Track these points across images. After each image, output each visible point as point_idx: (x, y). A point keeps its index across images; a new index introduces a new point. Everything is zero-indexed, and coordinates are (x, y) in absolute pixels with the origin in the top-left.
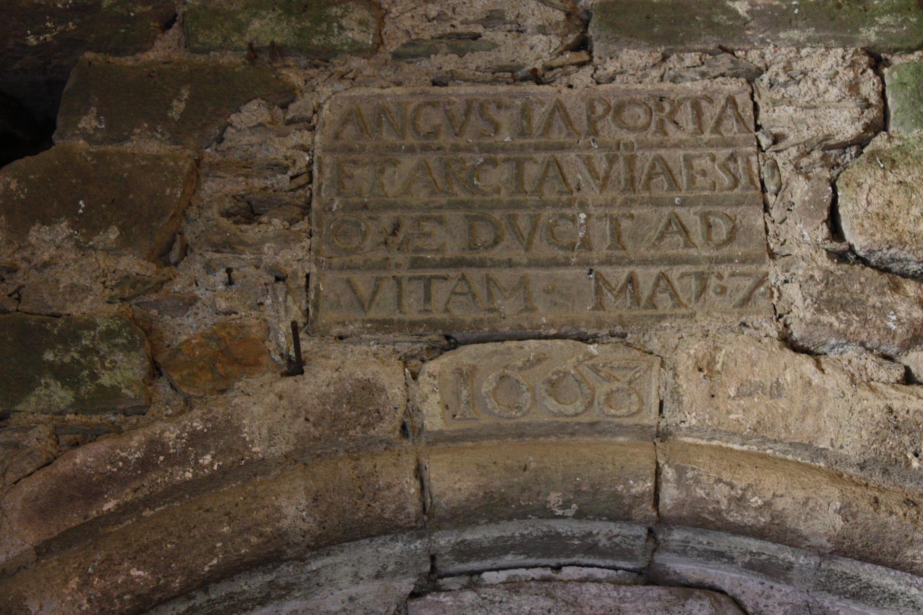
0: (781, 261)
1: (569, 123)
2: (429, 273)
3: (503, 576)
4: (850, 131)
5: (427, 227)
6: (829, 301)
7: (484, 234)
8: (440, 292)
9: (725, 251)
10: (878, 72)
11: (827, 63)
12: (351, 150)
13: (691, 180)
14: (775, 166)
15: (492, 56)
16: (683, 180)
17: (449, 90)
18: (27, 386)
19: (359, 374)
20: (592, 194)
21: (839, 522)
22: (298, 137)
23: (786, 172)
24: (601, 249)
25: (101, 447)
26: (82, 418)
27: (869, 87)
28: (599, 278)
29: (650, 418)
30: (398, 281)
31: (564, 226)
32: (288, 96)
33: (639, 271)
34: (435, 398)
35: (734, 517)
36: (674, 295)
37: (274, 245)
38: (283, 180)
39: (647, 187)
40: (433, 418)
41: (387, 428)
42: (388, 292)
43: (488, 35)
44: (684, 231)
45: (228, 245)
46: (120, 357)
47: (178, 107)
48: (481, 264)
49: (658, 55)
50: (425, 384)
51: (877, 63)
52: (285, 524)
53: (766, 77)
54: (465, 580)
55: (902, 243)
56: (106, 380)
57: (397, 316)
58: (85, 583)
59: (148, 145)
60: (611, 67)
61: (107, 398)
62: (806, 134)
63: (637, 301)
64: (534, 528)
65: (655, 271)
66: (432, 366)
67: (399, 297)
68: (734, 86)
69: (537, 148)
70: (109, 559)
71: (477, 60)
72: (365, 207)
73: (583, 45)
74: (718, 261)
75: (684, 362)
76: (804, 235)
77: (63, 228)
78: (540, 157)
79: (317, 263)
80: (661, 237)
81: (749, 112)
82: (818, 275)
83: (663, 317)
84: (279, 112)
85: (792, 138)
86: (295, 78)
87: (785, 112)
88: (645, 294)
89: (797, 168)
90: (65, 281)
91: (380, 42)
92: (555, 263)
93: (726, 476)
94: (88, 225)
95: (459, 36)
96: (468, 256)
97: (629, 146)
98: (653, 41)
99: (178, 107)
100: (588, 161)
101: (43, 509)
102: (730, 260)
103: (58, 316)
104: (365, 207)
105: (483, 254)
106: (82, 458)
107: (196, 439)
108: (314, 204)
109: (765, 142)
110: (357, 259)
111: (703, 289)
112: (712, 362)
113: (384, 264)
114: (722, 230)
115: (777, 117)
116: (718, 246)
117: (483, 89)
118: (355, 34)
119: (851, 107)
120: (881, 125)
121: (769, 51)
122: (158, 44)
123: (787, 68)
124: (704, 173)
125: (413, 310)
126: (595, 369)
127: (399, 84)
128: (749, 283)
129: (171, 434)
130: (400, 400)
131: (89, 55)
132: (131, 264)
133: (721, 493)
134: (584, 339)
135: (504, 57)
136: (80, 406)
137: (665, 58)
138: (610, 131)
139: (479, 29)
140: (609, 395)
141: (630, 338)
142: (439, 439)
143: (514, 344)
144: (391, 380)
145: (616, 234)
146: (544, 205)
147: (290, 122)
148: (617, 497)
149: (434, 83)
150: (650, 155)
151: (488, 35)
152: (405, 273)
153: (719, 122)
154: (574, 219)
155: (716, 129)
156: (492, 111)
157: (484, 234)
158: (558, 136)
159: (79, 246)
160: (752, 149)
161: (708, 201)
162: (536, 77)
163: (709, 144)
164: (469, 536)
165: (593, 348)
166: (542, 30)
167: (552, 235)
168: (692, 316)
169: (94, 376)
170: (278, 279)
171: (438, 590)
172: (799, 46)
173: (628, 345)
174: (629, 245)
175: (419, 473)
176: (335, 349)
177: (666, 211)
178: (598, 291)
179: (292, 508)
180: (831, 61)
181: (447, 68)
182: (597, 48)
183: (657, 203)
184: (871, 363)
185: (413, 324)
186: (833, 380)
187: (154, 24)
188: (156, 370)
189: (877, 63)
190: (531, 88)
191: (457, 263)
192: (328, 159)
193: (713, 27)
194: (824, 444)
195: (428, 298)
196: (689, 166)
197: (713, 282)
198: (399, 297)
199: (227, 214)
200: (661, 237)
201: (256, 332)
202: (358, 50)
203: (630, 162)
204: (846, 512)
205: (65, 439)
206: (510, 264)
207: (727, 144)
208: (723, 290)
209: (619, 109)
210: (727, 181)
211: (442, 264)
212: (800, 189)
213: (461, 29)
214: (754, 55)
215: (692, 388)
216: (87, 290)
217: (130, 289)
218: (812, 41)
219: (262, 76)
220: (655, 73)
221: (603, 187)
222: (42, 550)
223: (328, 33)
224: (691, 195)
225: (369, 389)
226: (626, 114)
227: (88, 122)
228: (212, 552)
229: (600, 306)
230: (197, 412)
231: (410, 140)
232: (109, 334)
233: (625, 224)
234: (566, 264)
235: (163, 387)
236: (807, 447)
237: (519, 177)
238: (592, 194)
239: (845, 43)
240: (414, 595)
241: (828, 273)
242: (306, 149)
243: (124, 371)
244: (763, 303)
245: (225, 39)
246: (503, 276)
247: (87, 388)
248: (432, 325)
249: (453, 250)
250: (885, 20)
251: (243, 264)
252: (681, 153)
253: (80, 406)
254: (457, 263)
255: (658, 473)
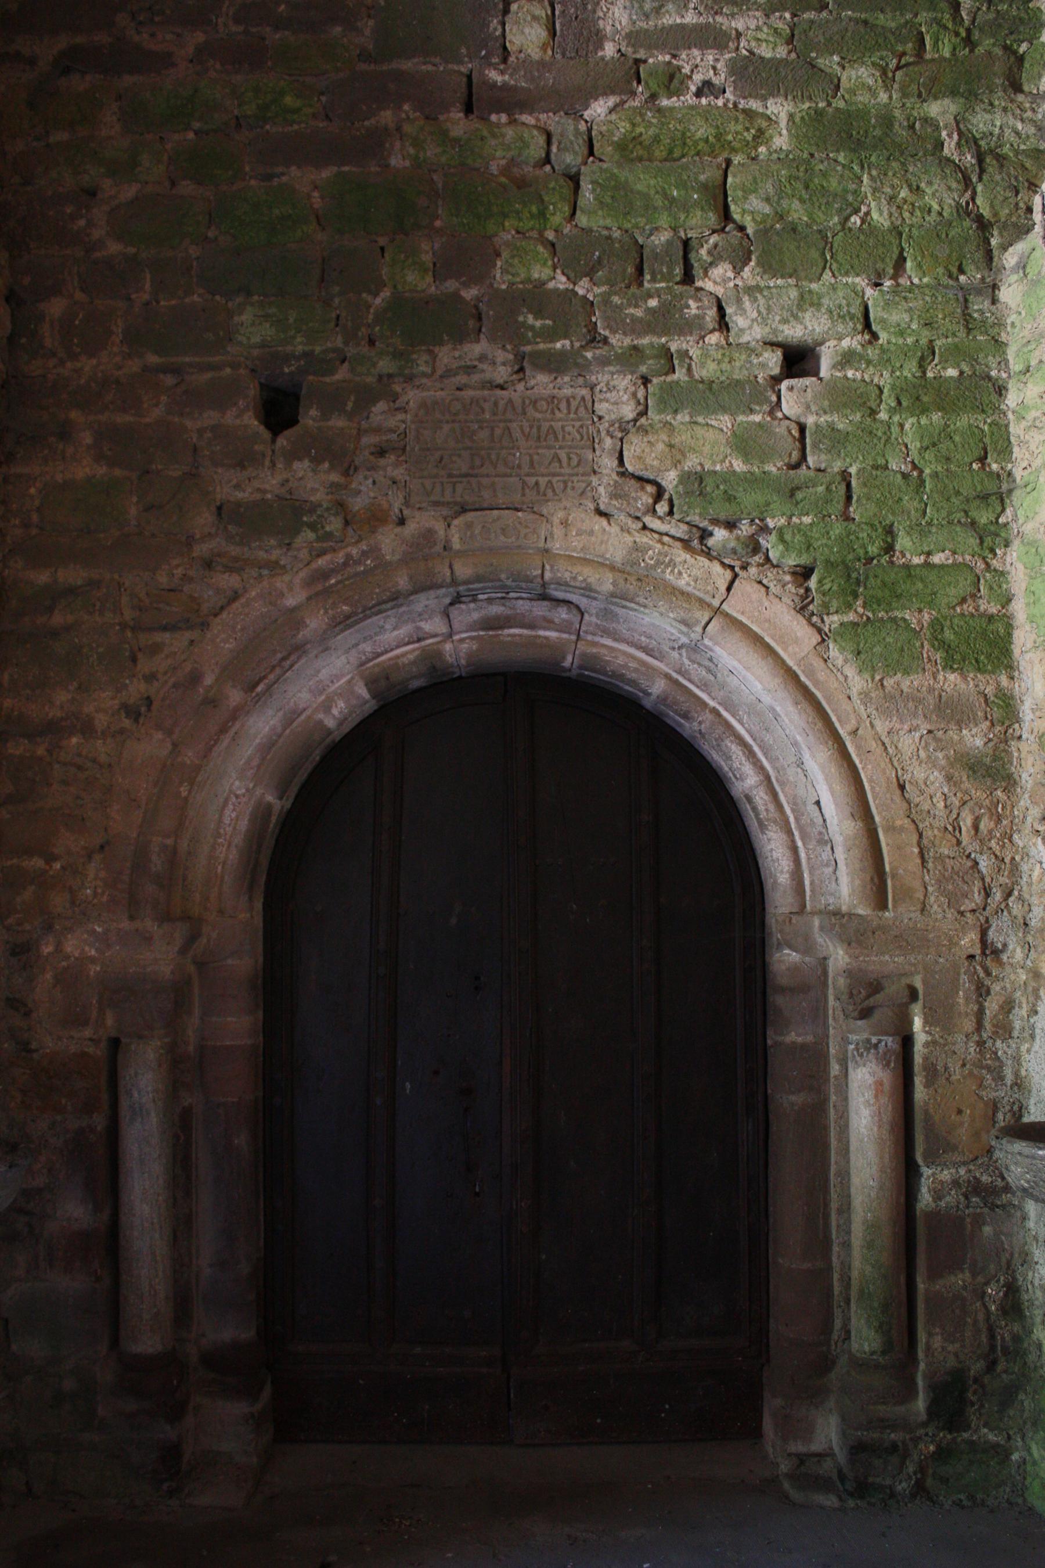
0: (598, 476)
1: (514, 409)
2: (455, 480)
3: (486, 596)
4: (631, 416)
5: (454, 458)
6: (615, 495)
7: (478, 462)
8: (459, 488)
9: (576, 470)
10: (646, 387)
11: (624, 382)
12: (422, 422)
13: (564, 437)
14: (599, 431)
15: (482, 376)
16: (560, 437)
17: (463, 393)
18: (298, 532)
19: (427, 525)
20: (522, 442)
21: (611, 587)
22: (400, 416)
23: (603, 434)
24: (526, 469)
25: (328, 557)
26: (320, 544)
27: (641, 394)
28: (524, 482)
29: (541, 544)
30: (442, 484)
31: (511, 458)
32: (395, 397)
33: (540, 479)
34: (457, 536)
35: (572, 583)
36: (554, 491)
37: (392, 468)
38: (394, 436)
39: (545, 440)
40: (456, 544)
41: (439, 548)
42: (438, 489)
43: (481, 366)
44: (560, 461)
45: (373, 468)
46: (332, 518)
47: (350, 405)
48: (476, 476)
49: (552, 378)
50: (453, 530)
51: (646, 381)
52: (400, 587)
53: (598, 387)
54: (470, 598)
55: (647, 470)
56: (328, 529)
57: (442, 500)
58: (326, 612)
59: (338, 422)
60: (532, 382)
61: (329, 536)
62: (613, 417)
63: (538, 492)
64: (498, 584)
65: (546, 479)
66: (456, 522)
67: (443, 491)
68: (585, 392)
69: (500, 421)
70: (334, 603)
71: (476, 378)
72: (428, 449)
73: (521, 370)
74: (573, 475)
75: (556, 521)
76: (608, 463)
77: (306, 463)
78: (502, 425)
79: (409, 475)
80: (550, 464)
81: (590, 404)
82: (612, 483)
83: (548, 501)
84: (392, 404)
85: (607, 418)
86: (397, 388)
87: (605, 405)
88: (542, 489)
89: (608, 432)
90: (309, 486)
91: (434, 371)
92: (506, 475)
93: (569, 569)
94: (317, 461)
95: (468, 367)
96: (471, 471)
97: (539, 420)
98: (550, 371)
99: (350, 405)
100: (521, 427)
101: (308, 583)
102: (577, 475)
103: (306, 501)
104: (428, 449)
105: (476, 471)
106: (321, 562)
107: (364, 553)
108: (408, 448)
109: (596, 419)
110: (425, 473)
111: (566, 487)
112: (567, 520)
113: (436, 476)
114: (574, 462)
115: (601, 408)
116: (573, 468)
117: (478, 392)
118: (423, 368)
119: (632, 405)
120: (644, 413)
121: (600, 376)
122: (340, 371)
123: (607, 384)
124: (569, 434)
125: (448, 498)
126: (520, 523)
127: (442, 389)
128: (584, 485)
129: (354, 551)
130: (443, 537)
131: (311, 378)
132: (335, 477)
133: (567, 575)
134: (517, 510)
135: (488, 376)
136: (319, 539)
137: (556, 378)
138: (531, 411)
139: (476, 363)
140: (526, 535)
141: (535, 509)
142: (460, 554)
143: (488, 512)
144: (440, 527)
145: (532, 462)
146: (503, 448)
147: (397, 409)
148: (527, 576)
149: (459, 389)
150: (547, 424)
151: (481, 366)
152: (445, 480)
153: (577, 409)
154: (514, 455)
155: (576, 413)
156: (481, 402)
157: (478, 462)
158: (509, 415)
159: (313, 470)
160: (590, 422)
161: (570, 447)
162: (502, 387)
163: (572, 420)
164: (471, 586)
165: (520, 514)
166: (504, 364)
167: (506, 464)
168: (560, 500)
169: (323, 527)
170: (394, 483)
171: (460, 602)
172: (613, 374)
173: (534, 512)
174: (537, 466)
175: (451, 567)
176: (417, 514)
177: (552, 451)
178: (523, 488)
179: (402, 582)
180: (626, 382)
181: (463, 382)
182: (528, 372)
183: (549, 448)
184: (630, 521)
185: (448, 503)
186: (614, 529)
187: (338, 363)
188: (347, 523)
189: (646, 381)
190: (499, 393)
191: (466, 475)
192: (413, 426)
193: (577, 365)
194: (608, 556)
195: (454, 492)
196: (563, 431)
197: (570, 484)
198: (443, 491)
199: (372, 454)
200: (550, 464)
201: (385, 506)
202: (424, 375)
203: (539, 428)
204: (615, 584)
205: (314, 553)
206: (488, 476)
207: (580, 419)
208: (573, 488)
209: (536, 402)
210: (578, 437)
211: (461, 476)
212: (608, 442)
213: (469, 363)
214: (593, 378)
215: (558, 531)
216: (317, 490)
217: (334, 487)
218: (618, 372)
219: (384, 389)
220: (551, 386)
221: (527, 440)
222: (309, 599)
223: (412, 368)
224: (564, 444)
225: (430, 532)
226: (538, 404)
227: (313, 412)
228: (372, 599)
229: (524, 495)
230: (364, 542)
231: (447, 417)
232: (328, 509)
233: (535, 457)
234: (511, 476)
235: (350, 531)
236: (602, 556)
237: (492, 435)
238: (522, 442)
239: (632, 373)
240: (451, 604)
241: (616, 482)
242: (403, 422)
243: (334, 524)
244: (589, 494)
245: (368, 370)
246: (485, 481)
247: (321, 532)
248: (456, 503)
249: (464, 469)
250: (651, 362)
251: (379, 476)
252: (560, 424)
253: (319, 539)
254: (466, 475)
255: (543, 566)
